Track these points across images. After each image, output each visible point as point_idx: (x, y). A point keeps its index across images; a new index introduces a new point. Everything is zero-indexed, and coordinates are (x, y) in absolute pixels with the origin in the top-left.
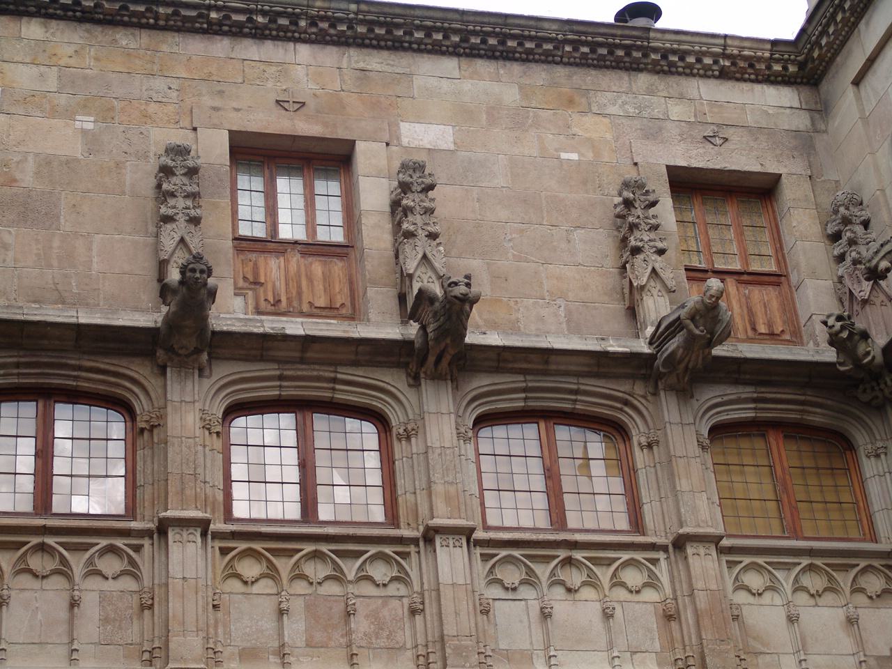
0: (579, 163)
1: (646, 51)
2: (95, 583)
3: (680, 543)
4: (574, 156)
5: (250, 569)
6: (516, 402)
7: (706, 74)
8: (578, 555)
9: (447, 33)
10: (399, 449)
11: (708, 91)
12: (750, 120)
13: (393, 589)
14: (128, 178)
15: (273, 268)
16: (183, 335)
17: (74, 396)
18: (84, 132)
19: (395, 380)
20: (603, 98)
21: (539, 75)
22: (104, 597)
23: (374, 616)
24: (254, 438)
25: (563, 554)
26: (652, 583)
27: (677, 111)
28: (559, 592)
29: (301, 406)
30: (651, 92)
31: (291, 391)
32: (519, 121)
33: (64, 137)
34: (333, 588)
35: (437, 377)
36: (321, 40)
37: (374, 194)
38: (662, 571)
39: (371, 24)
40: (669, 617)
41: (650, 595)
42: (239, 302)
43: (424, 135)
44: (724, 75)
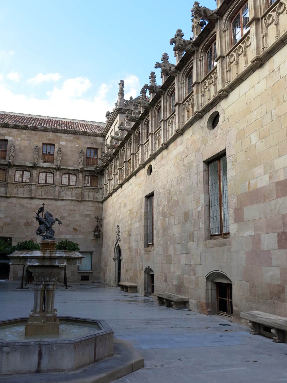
0: (78, 146)
1: (87, 134)
3: (78, 187)
4: (77, 146)
5: (40, 188)
6: (66, 173)
8: (69, 188)
10: (54, 177)
13: (52, 190)
14: (32, 148)
15: (46, 157)
17: (25, 171)
18: (28, 143)
19: (55, 171)
20: (81, 139)
21: (75, 136)
22: (27, 190)
24: (42, 175)
25: (68, 188)
26: (76, 191)
28: (67, 191)
29: (46, 172)
30: (87, 138)
32: (72, 141)
33: (26, 143)
34: (47, 190)
35: (58, 171)
36: (53, 132)
37: (56, 150)
38: (77, 190)
39: (58, 131)
41: (76, 192)
42: (42, 161)
43: (62, 143)
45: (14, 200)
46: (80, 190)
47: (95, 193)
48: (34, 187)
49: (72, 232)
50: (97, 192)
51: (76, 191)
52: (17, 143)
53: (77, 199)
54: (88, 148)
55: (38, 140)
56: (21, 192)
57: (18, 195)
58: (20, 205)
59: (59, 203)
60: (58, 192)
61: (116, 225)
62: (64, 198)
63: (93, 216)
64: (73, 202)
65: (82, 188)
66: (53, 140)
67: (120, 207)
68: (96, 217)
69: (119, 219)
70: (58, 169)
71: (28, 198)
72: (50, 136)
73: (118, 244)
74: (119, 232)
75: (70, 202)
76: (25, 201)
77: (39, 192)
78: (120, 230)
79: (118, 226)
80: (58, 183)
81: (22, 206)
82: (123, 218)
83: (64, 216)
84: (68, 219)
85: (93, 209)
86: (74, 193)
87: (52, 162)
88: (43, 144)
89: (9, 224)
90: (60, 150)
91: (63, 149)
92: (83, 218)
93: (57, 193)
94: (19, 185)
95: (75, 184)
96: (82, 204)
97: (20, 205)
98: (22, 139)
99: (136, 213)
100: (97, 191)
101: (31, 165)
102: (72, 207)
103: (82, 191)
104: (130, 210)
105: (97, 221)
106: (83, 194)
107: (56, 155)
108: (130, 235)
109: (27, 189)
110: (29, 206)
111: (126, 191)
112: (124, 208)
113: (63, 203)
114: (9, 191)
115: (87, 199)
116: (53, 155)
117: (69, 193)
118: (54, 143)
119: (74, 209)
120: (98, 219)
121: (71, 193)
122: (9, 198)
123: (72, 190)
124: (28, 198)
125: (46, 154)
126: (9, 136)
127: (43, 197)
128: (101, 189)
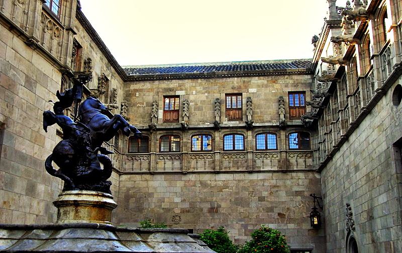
2: (207, 159)
5: (226, 157)
7: (296, 74)
9: (256, 74)
11: (295, 77)
12: (302, 82)
15: (231, 113)
16: (217, 127)
23: (241, 162)
26: (277, 157)
27: (291, 81)
31: (231, 132)
32: (267, 86)
33: (203, 97)
34: (236, 159)
36: (238, 77)
37: (244, 101)
40: (279, 161)
41: (277, 158)
43: (252, 90)
44: (299, 74)
45: (192, 177)
46: (284, 155)
47: (307, 158)
48: (217, 157)
49: (278, 219)
50: (310, 157)
51: (277, 158)
52: (192, 98)
53: (281, 170)
54: (290, 93)
55: (219, 89)
56: (200, 165)
57: (197, 169)
58: (201, 183)
59: (254, 177)
60: (252, 162)
61: (345, 204)
62: (262, 170)
63: (307, 194)
64: (275, 174)
65: (286, 152)
66: (240, 87)
67: (348, 173)
68: (311, 195)
69: (349, 194)
70: (249, 127)
71: (211, 173)
72: (235, 82)
73: (351, 234)
74: (351, 214)
75: (270, 174)
76: (206, 178)
77: (226, 163)
78: (353, 211)
79: (348, 205)
80: (250, 147)
81: (204, 184)
82: (356, 190)
83: (263, 195)
84: (269, 200)
85: (306, 182)
86: (276, 161)
87: (240, 119)
88: (227, 95)
89: (188, 211)
90: (249, 100)
91: (255, 100)
92: (292, 197)
93: (250, 163)
94: (197, 155)
95: (275, 148)
96: (289, 175)
97: (201, 183)
98: (197, 93)
99: (378, 177)
100: (309, 155)
101: (212, 126)
102: (274, 182)
103: (286, 156)
104: (367, 175)
105: (314, 201)
106: (289, 161)
107: (244, 108)
108: (371, 218)
109: (209, 160)
110: (213, 184)
111: (356, 145)
112: (356, 173)
113: (261, 176)
114: (185, 164)
115: (295, 169)
116: (241, 109)
117: (268, 161)
118: (241, 92)
119: (278, 185)
120: (315, 197)
121: (271, 161)
122: (186, 174)
123: (273, 157)
124: (211, 173)
125: (231, 109)
126: (181, 90)
127: (232, 170)
128: (315, 151)
